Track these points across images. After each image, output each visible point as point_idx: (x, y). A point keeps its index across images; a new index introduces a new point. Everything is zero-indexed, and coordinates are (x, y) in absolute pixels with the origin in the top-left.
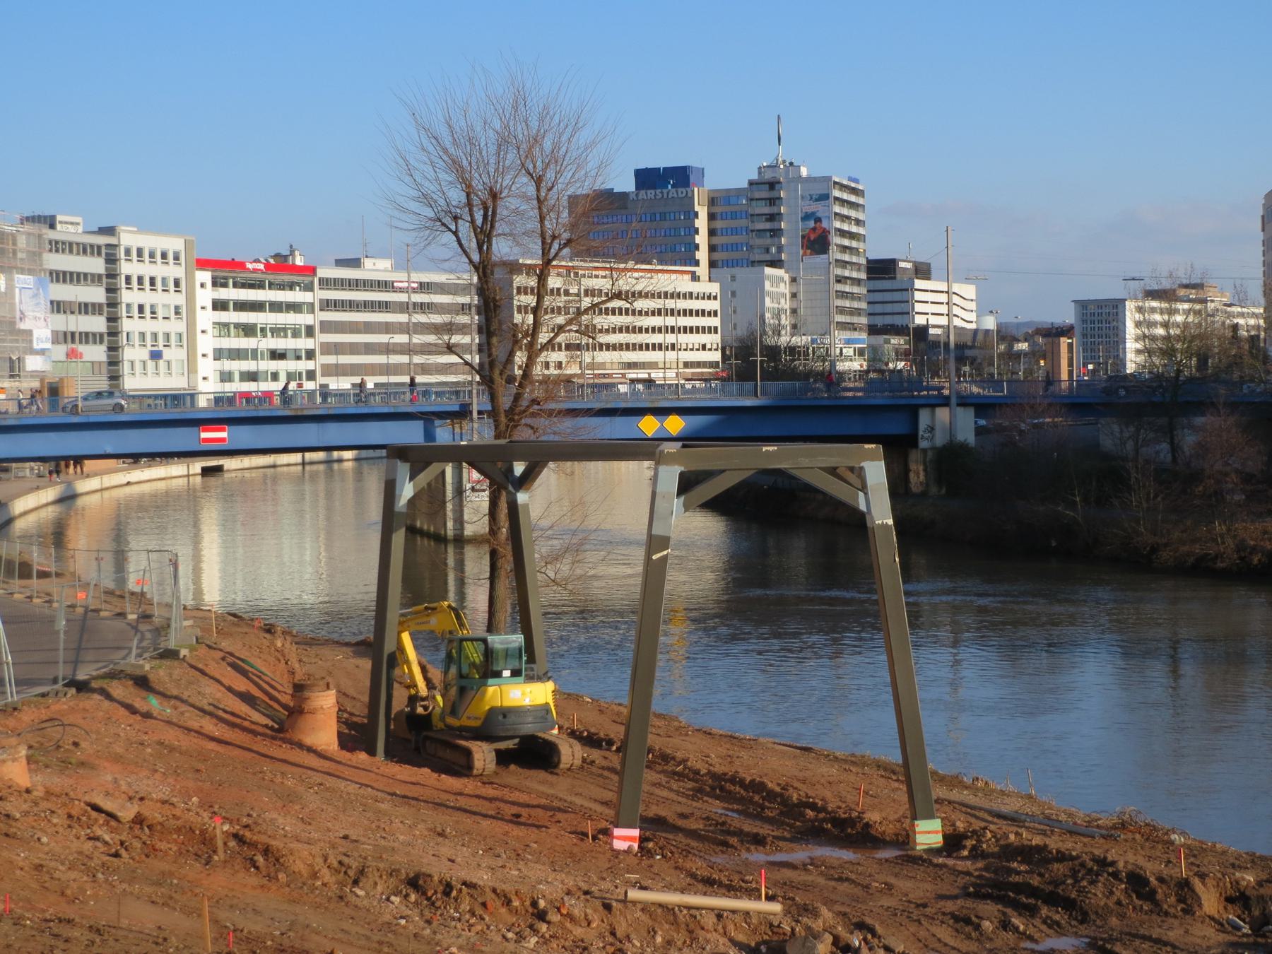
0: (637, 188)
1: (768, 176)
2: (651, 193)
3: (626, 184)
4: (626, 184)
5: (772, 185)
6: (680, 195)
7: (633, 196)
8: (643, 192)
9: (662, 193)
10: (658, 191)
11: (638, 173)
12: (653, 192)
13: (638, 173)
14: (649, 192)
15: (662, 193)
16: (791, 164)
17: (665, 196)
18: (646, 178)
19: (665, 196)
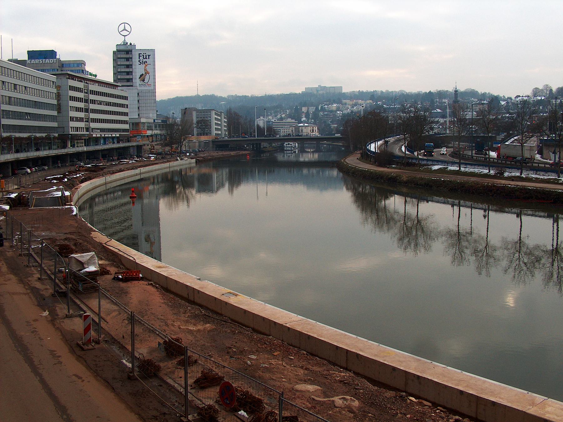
0: (29, 59)
1: (122, 48)
2: (37, 61)
3: (26, 57)
4: (26, 57)
5: (128, 52)
6: (51, 62)
7: (29, 62)
8: (33, 60)
9: (42, 61)
10: (40, 60)
11: (29, 52)
12: (38, 60)
13: (29, 52)
14: (36, 60)
15: (42, 61)
16: (131, 44)
17: (44, 62)
18: (32, 54)
19: (44, 62)
